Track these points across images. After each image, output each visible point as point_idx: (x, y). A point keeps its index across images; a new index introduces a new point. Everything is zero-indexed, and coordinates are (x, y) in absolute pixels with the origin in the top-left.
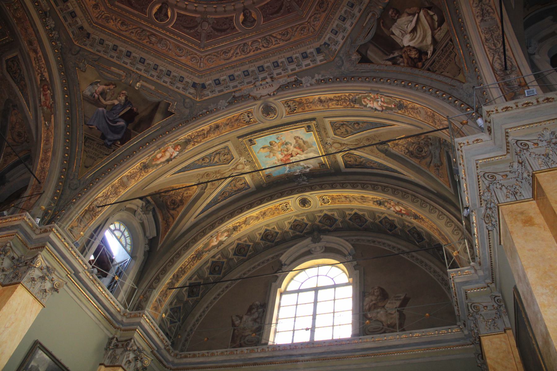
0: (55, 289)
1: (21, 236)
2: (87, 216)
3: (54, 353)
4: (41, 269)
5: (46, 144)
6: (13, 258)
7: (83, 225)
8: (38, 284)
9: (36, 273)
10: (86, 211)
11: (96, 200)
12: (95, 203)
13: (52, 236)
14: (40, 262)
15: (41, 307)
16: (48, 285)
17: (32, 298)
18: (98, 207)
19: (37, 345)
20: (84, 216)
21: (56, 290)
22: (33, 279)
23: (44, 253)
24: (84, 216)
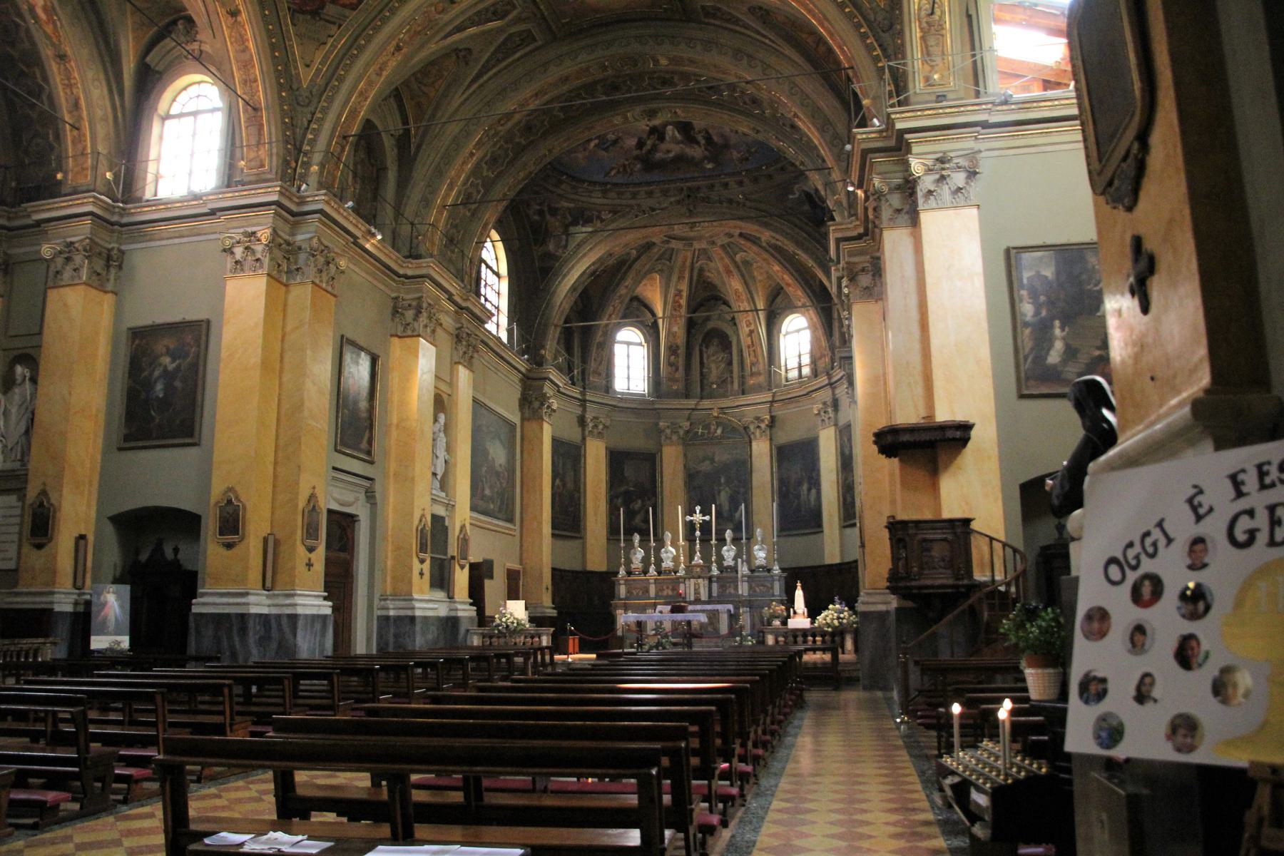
0: (972, 174)
1: (879, 158)
2: (932, 41)
3: (1049, 242)
4: (929, 170)
5: (814, 17)
6: (899, 187)
7: (938, 60)
8: (945, 191)
9: (927, 183)
10: (923, 38)
11: (920, 9)
12: (923, 13)
13: (899, 126)
14: (916, 166)
15: (974, 211)
16: (959, 179)
17: (951, 212)
18: (932, 13)
19: (1011, 257)
20: (927, 47)
21: (975, 173)
22: (930, 192)
23: (915, 149)
24: (927, 47)
